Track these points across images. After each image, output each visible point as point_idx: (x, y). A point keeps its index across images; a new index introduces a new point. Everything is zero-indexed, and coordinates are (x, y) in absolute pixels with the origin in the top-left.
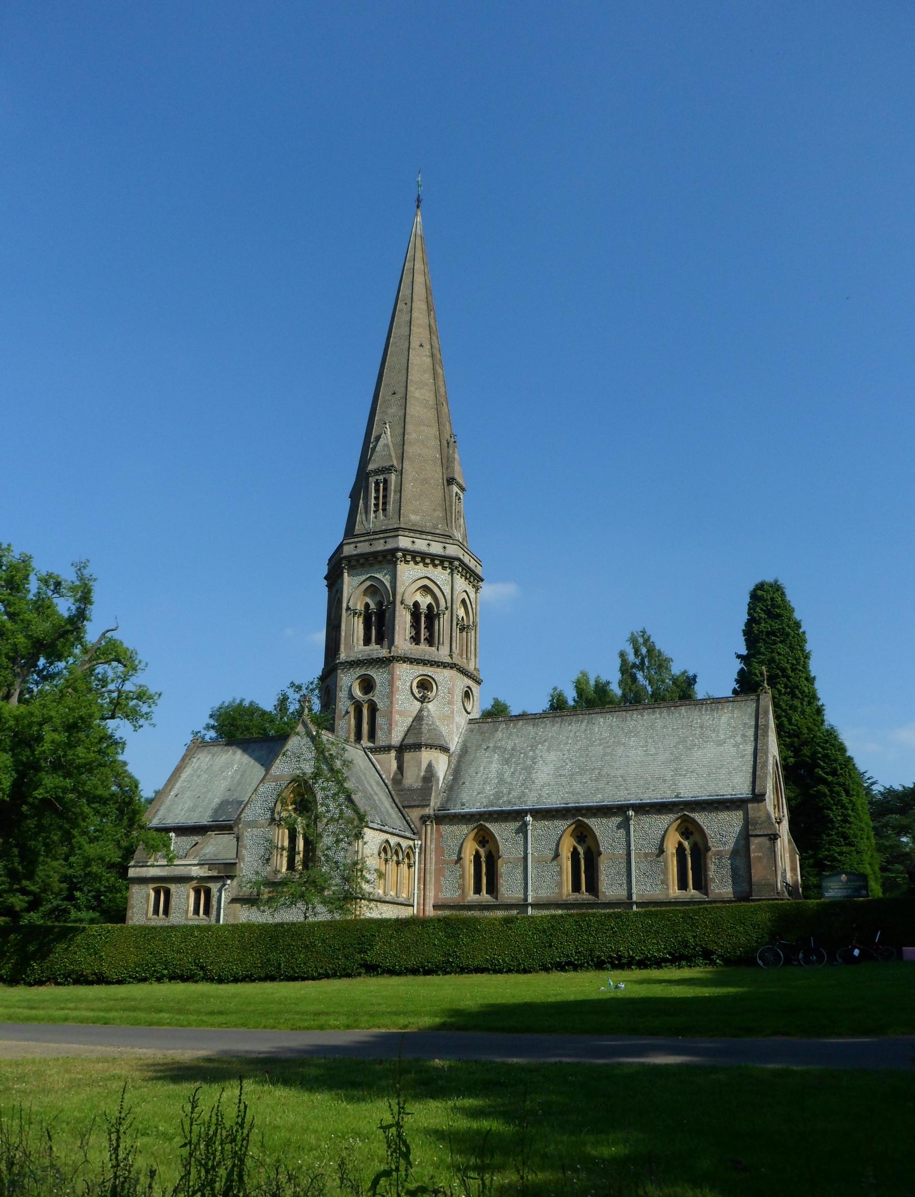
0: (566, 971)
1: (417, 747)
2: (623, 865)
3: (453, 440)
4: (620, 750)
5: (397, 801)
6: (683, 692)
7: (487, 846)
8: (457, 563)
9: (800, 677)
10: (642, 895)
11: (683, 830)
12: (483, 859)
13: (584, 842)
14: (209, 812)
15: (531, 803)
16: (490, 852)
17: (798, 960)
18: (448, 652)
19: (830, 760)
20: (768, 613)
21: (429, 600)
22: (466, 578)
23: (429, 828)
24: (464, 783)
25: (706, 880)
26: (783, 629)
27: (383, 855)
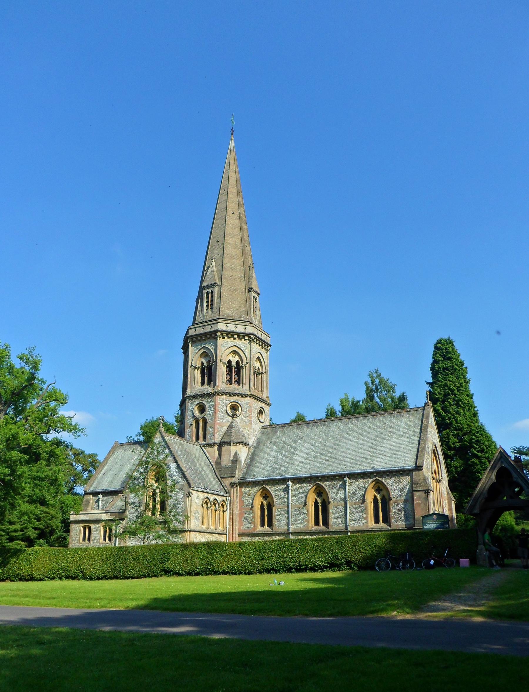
0: (271, 573)
1: (229, 443)
2: (343, 510)
3: (252, 266)
4: (343, 442)
5: (217, 474)
6: (400, 405)
7: (268, 499)
8: (253, 337)
9: (463, 394)
10: (353, 527)
11: (377, 488)
12: (265, 507)
13: (321, 496)
14: (120, 483)
15: (291, 474)
16: (269, 503)
17: (399, 567)
18: (248, 388)
19: (480, 443)
20: (444, 357)
21: (237, 358)
22: (260, 345)
23: (235, 489)
24: (256, 463)
25: (389, 518)
26: (453, 366)
27: (205, 506)
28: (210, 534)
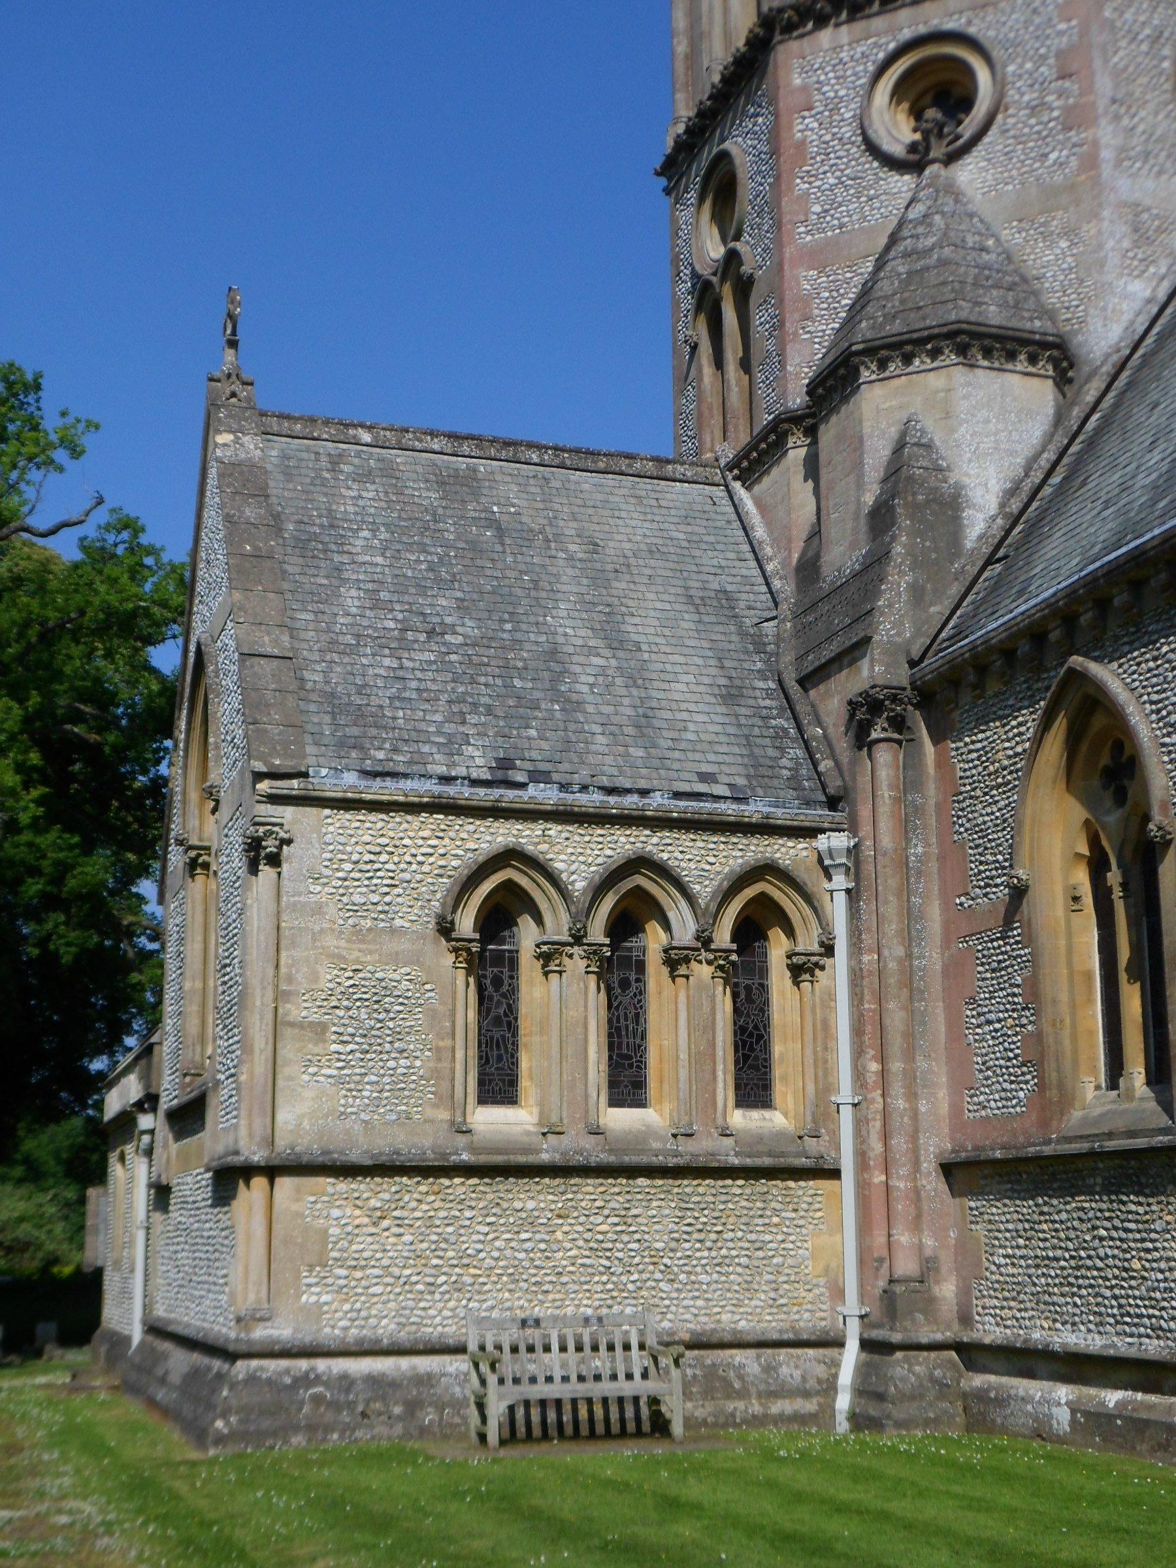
28: (590, 1185)
